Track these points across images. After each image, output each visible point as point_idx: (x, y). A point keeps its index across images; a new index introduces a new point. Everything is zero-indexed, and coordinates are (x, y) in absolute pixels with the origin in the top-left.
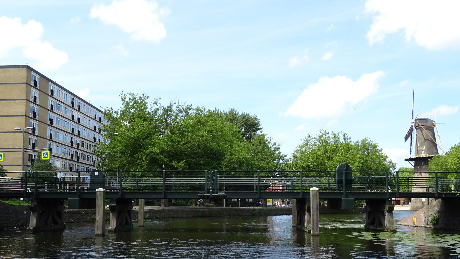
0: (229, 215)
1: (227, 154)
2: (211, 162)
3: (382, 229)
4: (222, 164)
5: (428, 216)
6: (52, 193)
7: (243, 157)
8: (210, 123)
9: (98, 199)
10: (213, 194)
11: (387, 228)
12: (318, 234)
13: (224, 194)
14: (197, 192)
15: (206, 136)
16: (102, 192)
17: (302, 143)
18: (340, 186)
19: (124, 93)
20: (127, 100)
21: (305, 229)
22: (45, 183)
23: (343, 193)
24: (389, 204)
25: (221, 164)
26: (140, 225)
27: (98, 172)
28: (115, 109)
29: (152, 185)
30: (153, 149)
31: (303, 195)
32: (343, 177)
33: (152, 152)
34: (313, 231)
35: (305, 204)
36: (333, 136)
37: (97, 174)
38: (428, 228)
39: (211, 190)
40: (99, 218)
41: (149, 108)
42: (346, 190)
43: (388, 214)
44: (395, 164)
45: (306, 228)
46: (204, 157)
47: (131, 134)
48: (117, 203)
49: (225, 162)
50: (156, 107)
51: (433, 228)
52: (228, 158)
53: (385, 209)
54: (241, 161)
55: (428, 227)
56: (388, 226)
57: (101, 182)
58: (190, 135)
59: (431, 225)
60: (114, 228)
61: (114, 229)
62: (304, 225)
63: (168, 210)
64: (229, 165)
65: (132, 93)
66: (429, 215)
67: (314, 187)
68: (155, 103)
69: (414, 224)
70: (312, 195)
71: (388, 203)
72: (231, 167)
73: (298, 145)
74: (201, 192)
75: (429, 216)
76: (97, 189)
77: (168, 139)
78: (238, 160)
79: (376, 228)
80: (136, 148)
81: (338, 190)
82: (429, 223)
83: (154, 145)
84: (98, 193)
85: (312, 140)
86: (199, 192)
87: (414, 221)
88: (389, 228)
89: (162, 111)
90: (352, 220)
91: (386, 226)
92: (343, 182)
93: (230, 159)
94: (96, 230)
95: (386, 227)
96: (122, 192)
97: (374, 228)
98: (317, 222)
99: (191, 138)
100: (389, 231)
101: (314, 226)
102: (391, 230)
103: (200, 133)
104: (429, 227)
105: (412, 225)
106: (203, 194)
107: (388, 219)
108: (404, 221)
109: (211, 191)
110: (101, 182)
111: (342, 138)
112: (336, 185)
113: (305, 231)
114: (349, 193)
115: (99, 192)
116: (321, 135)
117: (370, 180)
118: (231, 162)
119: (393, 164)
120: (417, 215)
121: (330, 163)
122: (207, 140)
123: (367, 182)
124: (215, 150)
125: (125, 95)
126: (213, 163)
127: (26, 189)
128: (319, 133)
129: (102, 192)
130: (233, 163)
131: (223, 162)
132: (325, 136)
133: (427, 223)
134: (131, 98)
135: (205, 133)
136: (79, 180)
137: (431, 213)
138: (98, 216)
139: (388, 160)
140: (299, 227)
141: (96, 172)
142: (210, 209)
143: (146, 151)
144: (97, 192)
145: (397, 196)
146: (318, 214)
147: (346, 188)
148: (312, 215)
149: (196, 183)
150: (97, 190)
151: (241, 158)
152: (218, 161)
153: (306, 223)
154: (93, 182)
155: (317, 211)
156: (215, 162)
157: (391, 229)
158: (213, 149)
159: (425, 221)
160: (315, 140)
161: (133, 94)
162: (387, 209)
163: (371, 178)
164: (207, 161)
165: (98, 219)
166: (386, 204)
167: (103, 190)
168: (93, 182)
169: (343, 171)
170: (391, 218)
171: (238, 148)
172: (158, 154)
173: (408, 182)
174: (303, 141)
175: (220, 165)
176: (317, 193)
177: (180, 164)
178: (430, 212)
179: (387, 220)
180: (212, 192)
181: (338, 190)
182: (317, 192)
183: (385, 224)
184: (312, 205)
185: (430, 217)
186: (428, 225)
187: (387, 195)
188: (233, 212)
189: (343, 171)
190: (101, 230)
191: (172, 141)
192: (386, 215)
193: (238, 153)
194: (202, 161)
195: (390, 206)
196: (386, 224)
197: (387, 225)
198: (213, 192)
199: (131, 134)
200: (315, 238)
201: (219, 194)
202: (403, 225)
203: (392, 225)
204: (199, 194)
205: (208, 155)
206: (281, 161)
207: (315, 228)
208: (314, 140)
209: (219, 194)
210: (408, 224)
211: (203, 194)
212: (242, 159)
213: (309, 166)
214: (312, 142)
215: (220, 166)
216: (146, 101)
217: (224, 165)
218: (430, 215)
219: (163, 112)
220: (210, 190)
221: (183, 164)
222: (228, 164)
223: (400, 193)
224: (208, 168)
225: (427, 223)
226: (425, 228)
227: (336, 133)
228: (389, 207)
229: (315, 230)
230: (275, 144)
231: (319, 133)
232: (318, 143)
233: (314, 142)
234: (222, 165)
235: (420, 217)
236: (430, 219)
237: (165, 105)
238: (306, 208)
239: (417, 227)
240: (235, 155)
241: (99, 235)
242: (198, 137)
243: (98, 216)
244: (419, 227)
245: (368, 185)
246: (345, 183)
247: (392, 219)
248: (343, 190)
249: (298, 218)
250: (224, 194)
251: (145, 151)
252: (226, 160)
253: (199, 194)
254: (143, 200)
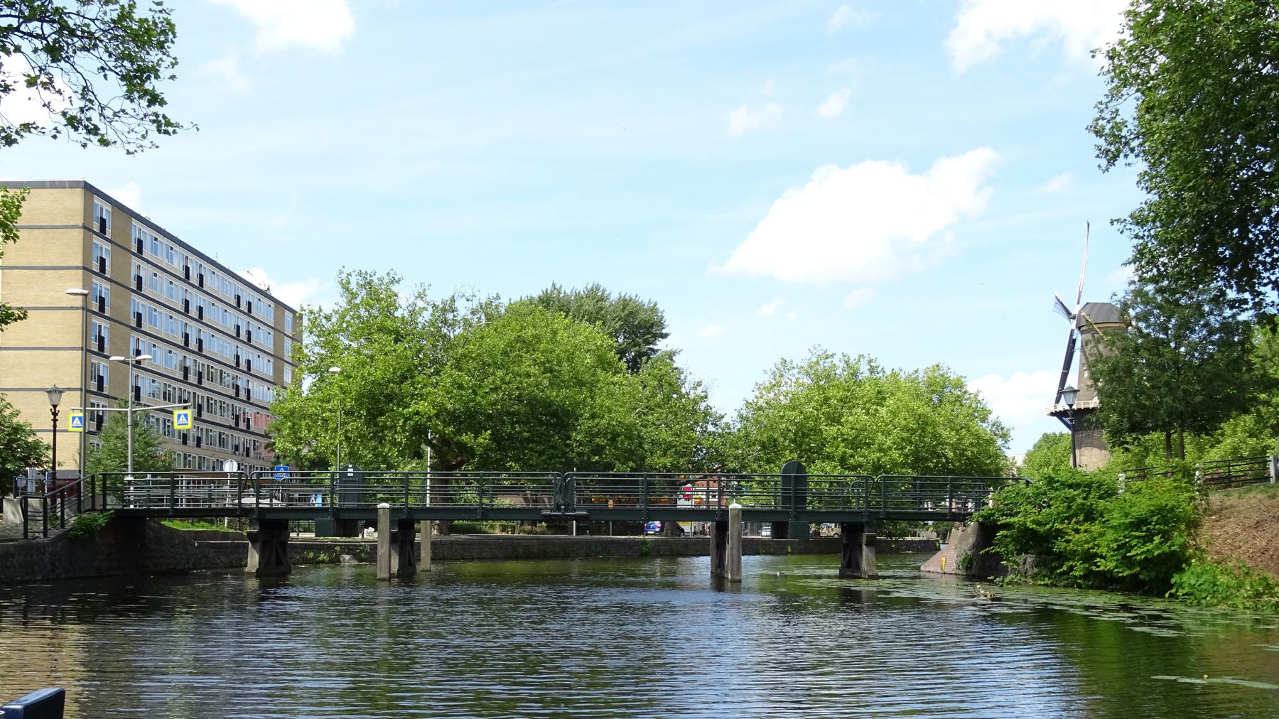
2: (546, 433)
11: (865, 573)
15: (535, 375)
17: (767, 379)
19: (346, 271)
20: (353, 286)
25: (569, 438)
28: (327, 310)
30: (423, 406)
33: (417, 413)
36: (842, 365)
41: (404, 307)
42: (796, 508)
44: (1008, 430)
47: (369, 374)
48: (399, 528)
50: (420, 304)
52: (585, 423)
58: (500, 373)
63: (452, 543)
65: (363, 272)
68: (421, 296)
73: (757, 384)
77: (454, 383)
80: (379, 401)
83: (422, 397)
84: (380, 512)
85: (791, 372)
89: (430, 310)
92: (790, 493)
99: (502, 380)
103: (524, 368)
109: (563, 507)
111: (864, 369)
116: (815, 360)
118: (591, 435)
119: (1003, 429)
121: (833, 430)
125: (350, 275)
126: (553, 436)
128: (809, 356)
129: (387, 511)
130: (597, 434)
132: (824, 362)
134: (361, 282)
135: (533, 370)
139: (991, 418)
140: (719, 571)
143: (403, 409)
147: (796, 504)
160: (799, 373)
161: (366, 273)
164: (537, 431)
172: (430, 418)
174: (770, 373)
177: (480, 440)
191: (461, 387)
198: (566, 510)
199: (369, 374)
206: (711, 428)
208: (795, 371)
213: (775, 440)
214: (792, 376)
215: (568, 442)
216: (395, 288)
219: (432, 315)
221: (485, 439)
227: (853, 357)
229: (735, 572)
230: (699, 384)
231: (809, 356)
232: (807, 381)
233: (797, 376)
237: (438, 296)
241: (383, 580)
248: (790, 508)
251: (401, 409)
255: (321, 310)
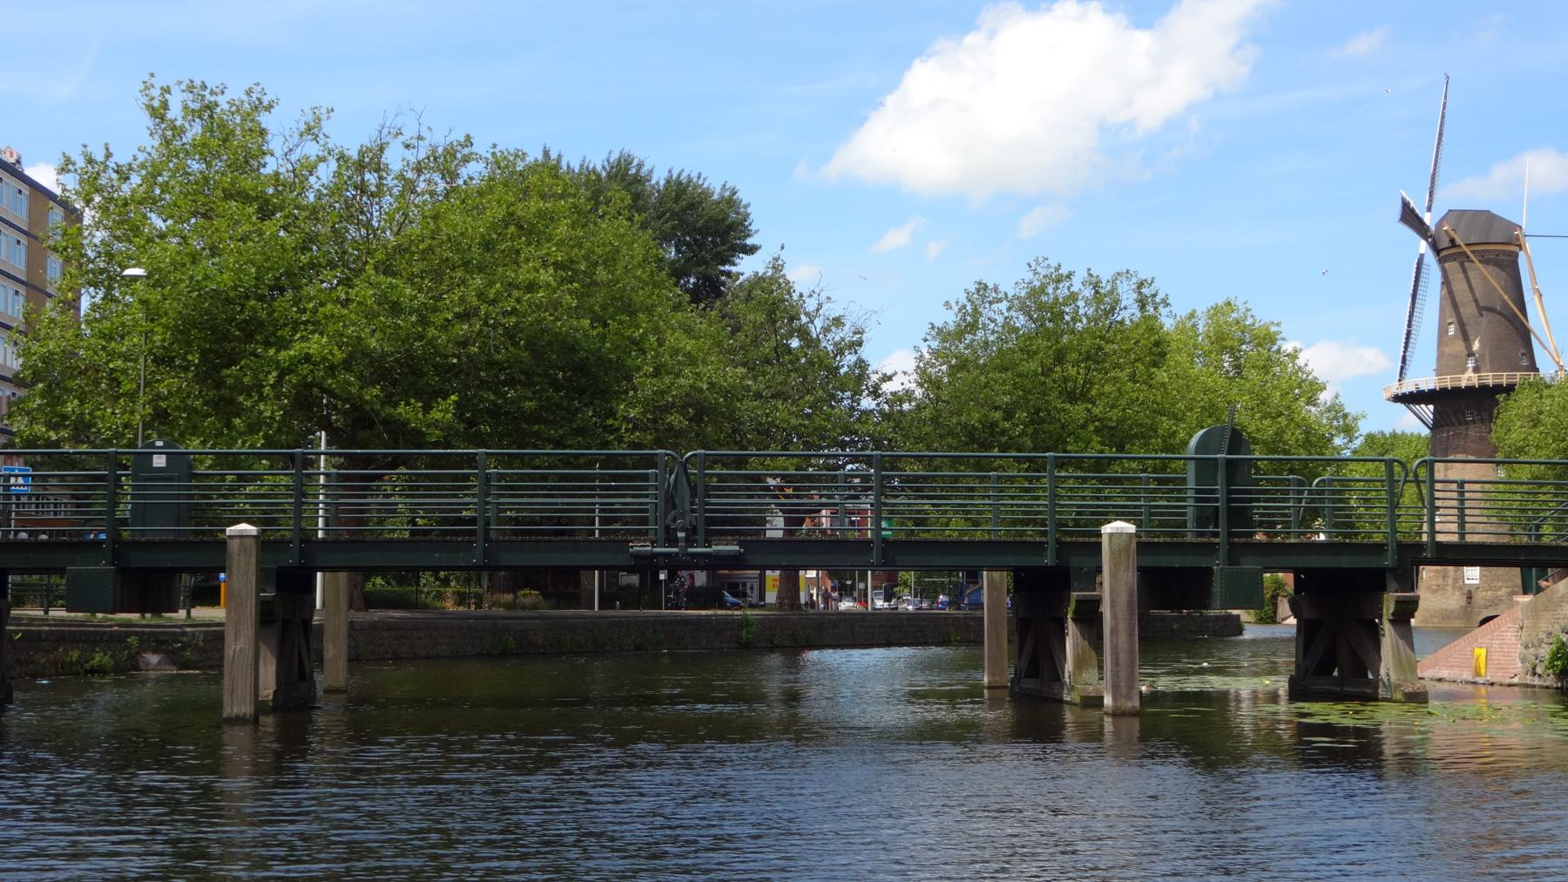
0: (638, 648)
1: (639, 369)
2: (565, 404)
3: (1369, 691)
4: (618, 416)
5: (1536, 642)
6: (202, 543)
7: (712, 385)
8: (563, 229)
9: (234, 570)
10: (690, 550)
11: (1388, 687)
12: (1134, 707)
13: (737, 548)
14: (622, 541)
15: (548, 285)
16: (253, 540)
17: (950, 319)
18: (1206, 517)
19: (159, 83)
20: (175, 112)
21: (1066, 692)
22: (824, 512)
23: (1218, 544)
24: (1396, 591)
25: (612, 414)
26: (330, 686)
27: (164, 456)
28: (122, 157)
29: (351, 511)
30: (316, 344)
31: (1058, 555)
32: (1215, 478)
33: (307, 358)
34: (1115, 699)
35: (1067, 587)
36: (1088, 292)
37: (159, 461)
38: (1537, 690)
39: (682, 531)
40: (238, 648)
41: (278, 153)
42: (1231, 535)
43: (1392, 630)
44: (1355, 419)
45: (1072, 688)
46: (534, 385)
47: (206, 277)
48: (279, 589)
49: (631, 405)
50: (311, 149)
51: (1556, 688)
52: (647, 387)
53: (1381, 609)
54: (706, 404)
55: (1534, 686)
56: (1393, 678)
57: (179, 496)
58: (478, 281)
59: (1549, 675)
60: (271, 692)
61: (271, 697)
62: (1057, 677)
63: (374, 626)
64: (648, 419)
65: (198, 83)
66: (1540, 636)
67: (1116, 520)
68: (311, 131)
69: (1478, 674)
70: (1112, 553)
71: (1392, 584)
72: (657, 430)
73: (933, 328)
74: (640, 541)
75: (1539, 639)
76: (228, 529)
77: (382, 300)
78: (687, 395)
79: (1339, 689)
80: (226, 337)
81: (1199, 534)
82: (1539, 670)
83: (317, 326)
84: (234, 546)
85: (995, 306)
86: (632, 542)
87: (1477, 659)
88: (1400, 685)
89: (333, 165)
90: (1205, 664)
91: (1385, 679)
92: (1216, 500)
93: (654, 393)
94: (226, 699)
95: (1384, 683)
96: (302, 541)
97: (1333, 688)
98: (1132, 661)
99: (481, 295)
100: (1399, 696)
101: (1118, 676)
102: (1406, 694)
103: (524, 276)
104: (1540, 683)
105: (1470, 678)
106: (649, 548)
107: (1393, 651)
108: (1436, 665)
109: (681, 535)
110: (179, 496)
111: (1128, 298)
112: (1190, 511)
113: (1061, 701)
114: (1243, 544)
115: (237, 541)
116: (1037, 284)
117: (1310, 492)
118: (656, 408)
119: (1345, 416)
120: (1489, 637)
121: (1078, 411)
122: (555, 305)
123: (1300, 501)
124: (587, 351)
125: (166, 90)
126: (577, 410)
127: (879, 529)
128: (1029, 276)
129: (251, 542)
130: (668, 408)
131: (622, 407)
132: (1057, 288)
133: (1534, 669)
134: (192, 106)
135: (546, 276)
136: (112, 488)
137: (1550, 629)
138: (236, 641)
139: (1325, 397)
141: (155, 456)
142: (552, 618)
143: (278, 351)
144: (228, 541)
145: (1429, 556)
146: (1134, 630)
147: (1230, 525)
148: (1112, 631)
149: (557, 504)
150: (231, 530)
151: (702, 389)
152: (597, 402)
153: (1069, 666)
154: (144, 497)
155: (1132, 615)
156: (586, 405)
157: (1407, 691)
158: (577, 348)
159: (1523, 661)
160: (1009, 309)
161: (204, 87)
162: (1391, 611)
163: (1317, 485)
164: (548, 399)
165: (237, 656)
166: (1383, 589)
167: (255, 533)
168: (144, 497)
169: (1218, 456)
170: (1407, 647)
171: (689, 345)
172: (332, 369)
173: (1462, 501)
174: (956, 309)
175: (608, 418)
176: (1129, 547)
177: (436, 415)
178: (1544, 625)
179: (1391, 653)
180: (687, 539)
181: (1199, 534)
182: (1130, 541)
183: (1383, 672)
184: (1111, 593)
185: (1543, 645)
186: (1536, 678)
187: (1390, 554)
188: (655, 631)
189: (1218, 456)
190: (248, 700)
191: (396, 309)
192: (1384, 635)
193: (689, 365)
194: (531, 400)
195: (1402, 599)
196: (1387, 667)
197: (1388, 675)
198: (689, 541)
199: (206, 277)
200: (1125, 722)
201: (715, 548)
202: (1432, 680)
203: (1409, 675)
204: (632, 547)
205: (550, 375)
206: (867, 403)
207: (1123, 684)
208: (1004, 306)
209: (715, 548)
210: (1453, 677)
211: (649, 548)
212: (707, 393)
213: (994, 425)
214: (996, 314)
215: (610, 422)
216: (265, 119)
217: (625, 418)
218: (1544, 636)
219: (338, 174)
220: (675, 530)
221: (447, 411)
222: (644, 414)
223: (1440, 545)
224: (552, 432)
225: (1534, 669)
226: (1524, 689)
227: (1105, 275)
228: (1399, 602)
229: (1124, 690)
230: (838, 322)
231: (1029, 276)
232: (1020, 320)
233: (1006, 314)
234: (616, 419)
235: (1501, 644)
236: (1546, 651)
237: (351, 138)
238: (1068, 605)
239: (1492, 684)
240: (678, 376)
241: (239, 721)
242: (516, 293)
243: (236, 641)
244: (1501, 685)
245: (1305, 511)
246: (1225, 506)
247: (1409, 651)
248: (1216, 535)
249: (1021, 651)
250: (737, 548)
251: (272, 352)
252: (634, 397)
253: (632, 547)
254: (345, 573)
255: (108, 155)
